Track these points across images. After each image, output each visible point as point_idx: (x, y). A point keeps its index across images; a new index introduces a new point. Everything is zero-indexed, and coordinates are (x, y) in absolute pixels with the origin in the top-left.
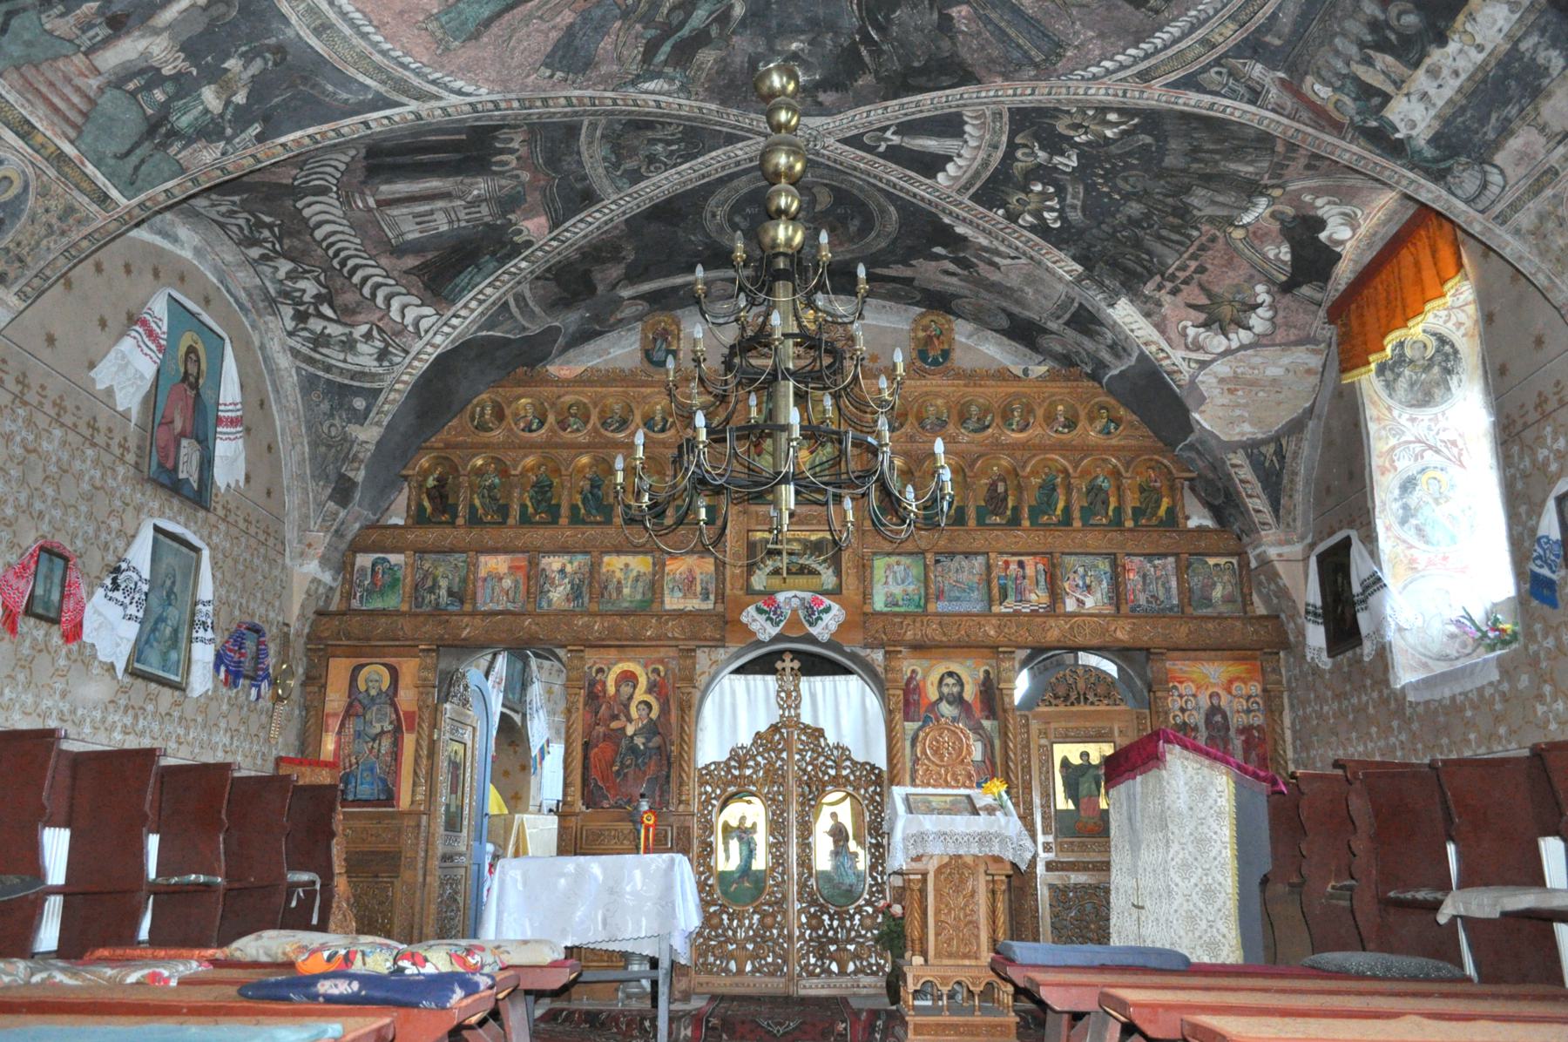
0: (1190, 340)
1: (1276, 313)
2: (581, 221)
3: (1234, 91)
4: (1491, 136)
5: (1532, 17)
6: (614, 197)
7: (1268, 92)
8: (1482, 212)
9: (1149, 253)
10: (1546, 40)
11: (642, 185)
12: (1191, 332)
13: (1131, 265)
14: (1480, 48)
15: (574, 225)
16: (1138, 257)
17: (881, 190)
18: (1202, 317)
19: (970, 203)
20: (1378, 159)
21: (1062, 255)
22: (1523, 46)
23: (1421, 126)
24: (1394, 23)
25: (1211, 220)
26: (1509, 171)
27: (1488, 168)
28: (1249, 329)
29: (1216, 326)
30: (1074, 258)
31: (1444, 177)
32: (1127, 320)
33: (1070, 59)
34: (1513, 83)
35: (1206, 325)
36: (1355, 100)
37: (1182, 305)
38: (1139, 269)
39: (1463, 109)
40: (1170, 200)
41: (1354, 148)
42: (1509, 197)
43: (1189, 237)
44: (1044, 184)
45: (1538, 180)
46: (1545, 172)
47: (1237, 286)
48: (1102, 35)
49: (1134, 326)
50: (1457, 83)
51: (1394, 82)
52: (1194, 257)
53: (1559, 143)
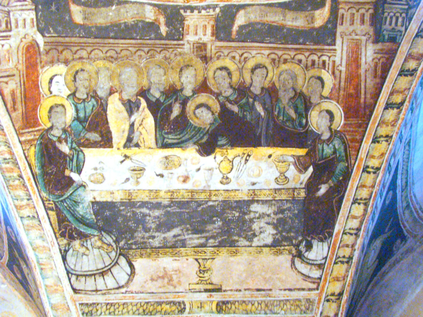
4: (156, 243)
5: (284, 197)
7: (7, 37)
8: (75, 291)
10: (274, 218)
14: (225, 180)
20: (27, 174)
22: (256, 208)
23: (105, 186)
24: (190, 106)
26: (137, 279)
27: (123, 261)
31: (72, 238)
34: (219, 223)
36: (77, 119)
39: (158, 206)
41: (18, 150)
42: (112, 298)
45: (160, 303)
46: (174, 303)
50: (177, 185)
51: (129, 140)
53: (206, 291)
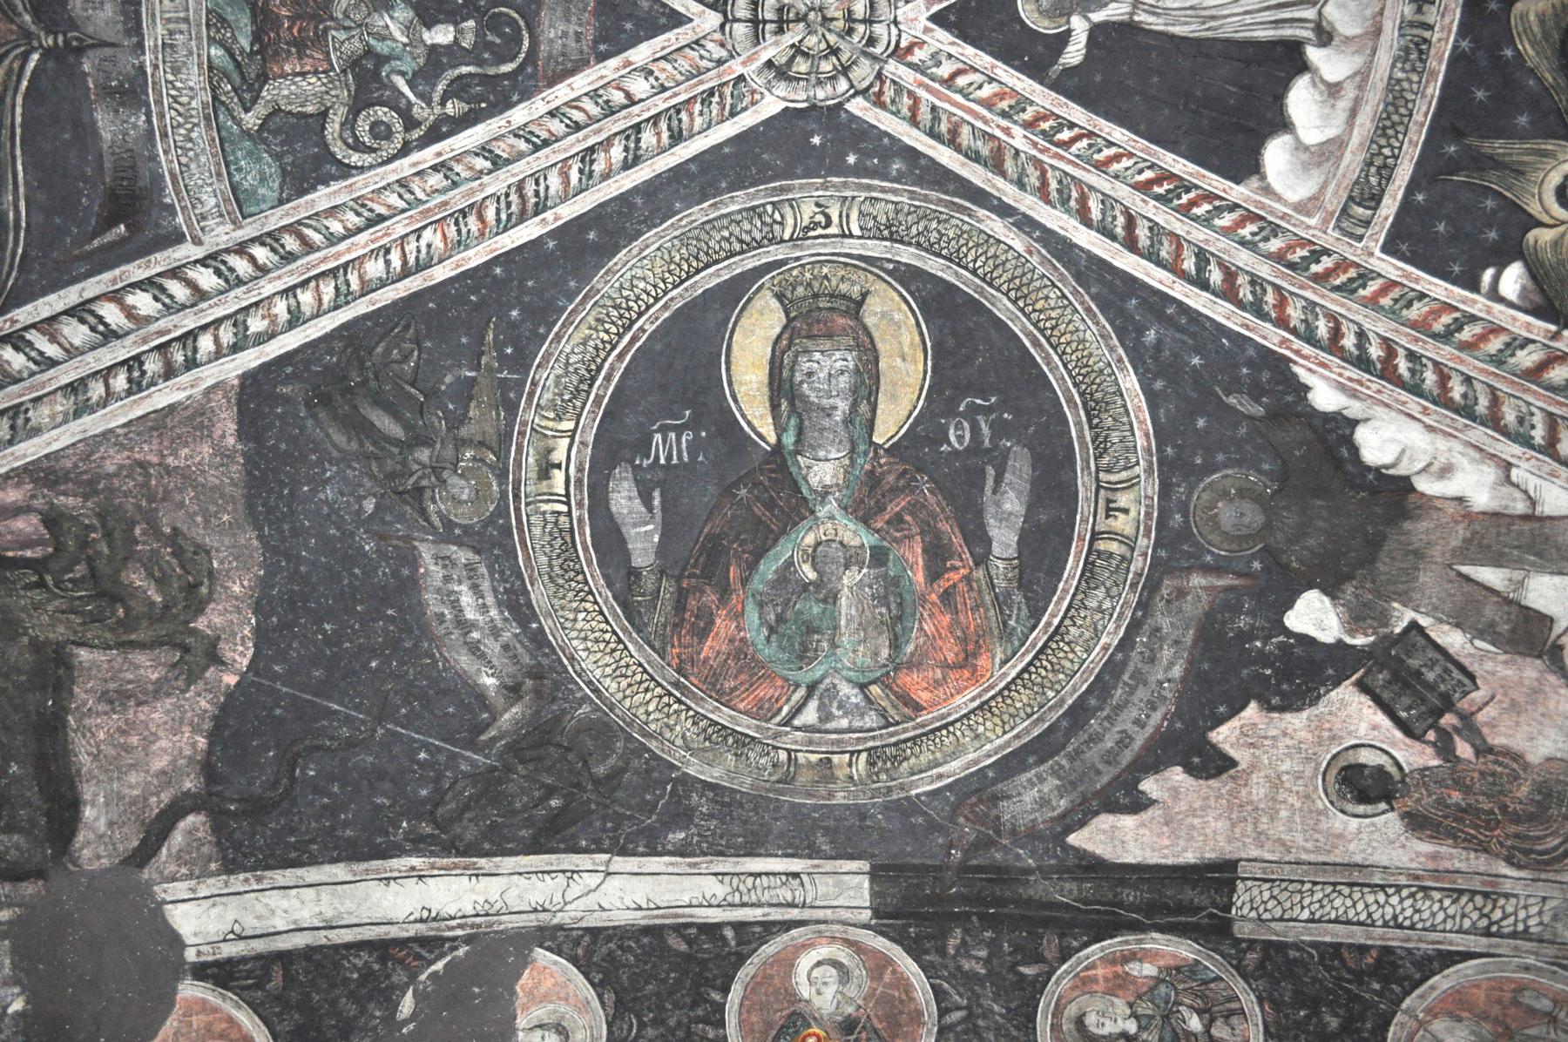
2: (79, 312)
6: (221, 235)
11: (322, 198)
15: (48, 326)
17: (1091, 271)
19: (1391, 267)
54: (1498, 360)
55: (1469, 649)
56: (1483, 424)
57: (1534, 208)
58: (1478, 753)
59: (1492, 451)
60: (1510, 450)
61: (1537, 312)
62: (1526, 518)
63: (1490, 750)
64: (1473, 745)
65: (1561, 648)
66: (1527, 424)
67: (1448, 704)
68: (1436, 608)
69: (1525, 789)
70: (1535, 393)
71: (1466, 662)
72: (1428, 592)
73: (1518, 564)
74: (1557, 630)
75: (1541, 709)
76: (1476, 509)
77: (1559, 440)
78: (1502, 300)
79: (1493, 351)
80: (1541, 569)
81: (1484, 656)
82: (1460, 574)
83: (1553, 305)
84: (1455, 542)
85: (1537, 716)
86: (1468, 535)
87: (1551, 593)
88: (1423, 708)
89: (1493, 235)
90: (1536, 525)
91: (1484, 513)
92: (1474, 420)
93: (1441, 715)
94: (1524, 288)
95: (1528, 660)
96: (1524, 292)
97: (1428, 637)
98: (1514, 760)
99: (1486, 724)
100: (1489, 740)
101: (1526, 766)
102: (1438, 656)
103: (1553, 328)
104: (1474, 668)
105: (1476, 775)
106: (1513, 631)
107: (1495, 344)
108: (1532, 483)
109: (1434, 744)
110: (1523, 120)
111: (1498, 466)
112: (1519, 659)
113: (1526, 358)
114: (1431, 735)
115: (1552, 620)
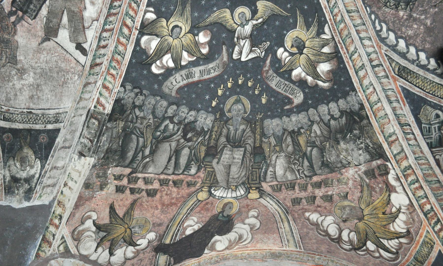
0: (81, 228)
1: (133, 258)
3: (429, 131)
9: (153, 152)
12: (89, 224)
13: (133, 145)
16: (145, 146)
18: (107, 221)
21: (117, 88)
25: (212, 175)
28: (111, 254)
29: (102, 234)
30: (118, 101)
32: (75, 175)
33: (396, 16)
35: (99, 227)
37: (110, 202)
38: (130, 154)
40: (223, 140)
43: (188, 167)
44: (209, 43)
47: (146, 221)
48: (429, 30)
49: (70, 183)
52: (163, 183)
54: (127, 14)
55: (43, 16)
56: (108, 12)
57: (172, 20)
58: (13, 23)
59: (101, 15)
60: (102, 20)
61: (142, 23)
62: (84, 27)
63: (15, 26)
64: (15, 21)
65: (49, 40)
66: (110, 23)
67: (25, 12)
68: (52, 6)
69: (7, 36)
70: (119, 25)
71: (39, 16)
72: (56, 3)
73: (70, 26)
74: (54, 39)
75: (31, 37)
76: (83, 13)
77: (106, 32)
78: (145, 13)
79: (129, 13)
80: (70, 33)
81: (42, 20)
82: (64, 11)
83: (145, 27)
84: (73, 8)
85: (28, 37)
86: (75, 12)
87: (64, 36)
88: (21, 6)
89: (163, 9)
90: (82, 30)
91: (83, 16)
92: (109, 9)
93: (21, 11)
94: (149, 19)
95: (44, 33)
96: (147, 19)
97: (43, 4)
98: (14, 33)
99: (22, 24)
100: (18, 25)
101: (13, 36)
102: (38, 8)
103: (139, 28)
104: (38, 19)
105: (6, 23)
106: (51, 27)
107: (132, 13)
108: (93, 27)
109: (12, 10)
110: (196, 14)
111: (97, 18)
112: (43, 30)
113: (129, 22)
114: (14, 9)
115: (56, 37)
